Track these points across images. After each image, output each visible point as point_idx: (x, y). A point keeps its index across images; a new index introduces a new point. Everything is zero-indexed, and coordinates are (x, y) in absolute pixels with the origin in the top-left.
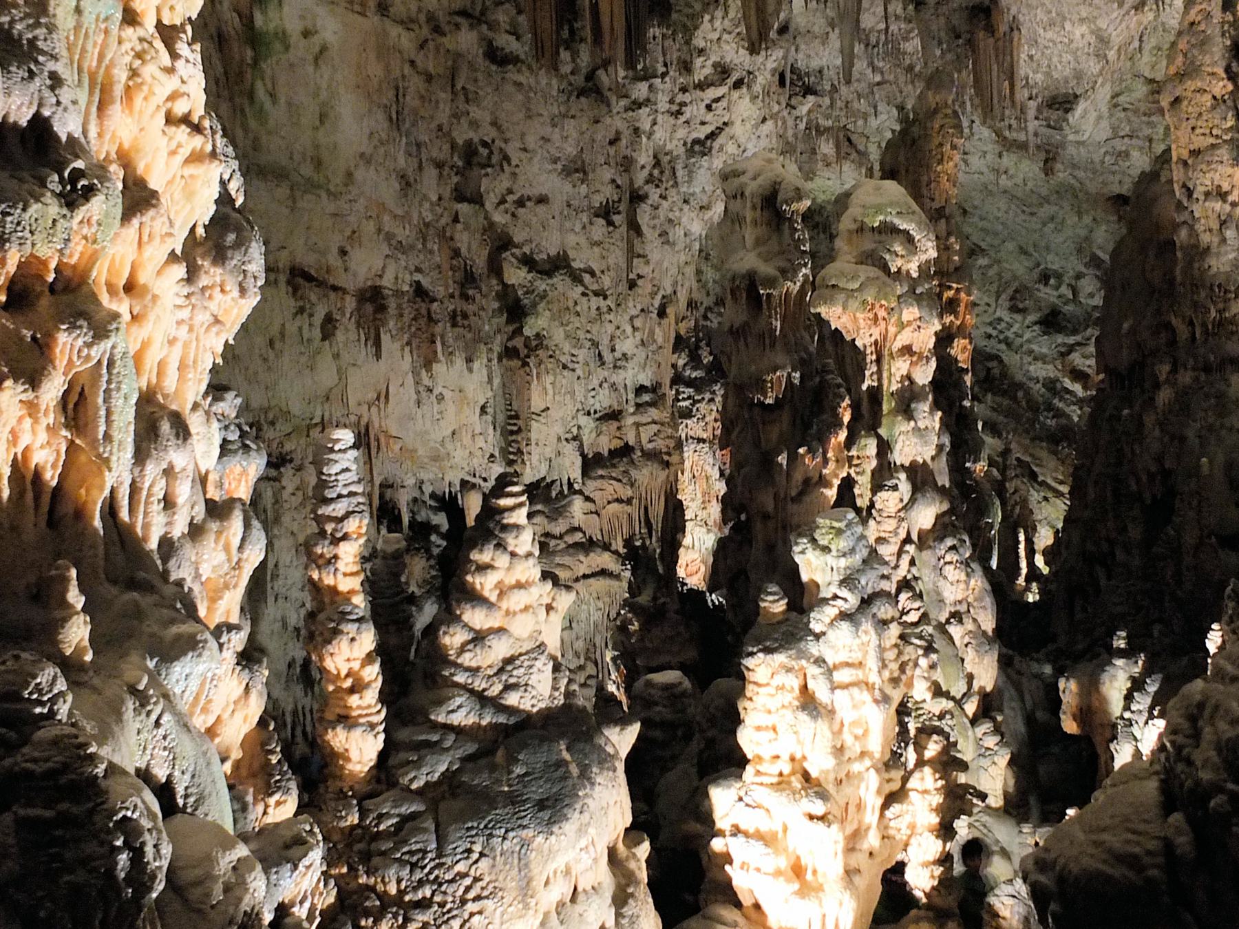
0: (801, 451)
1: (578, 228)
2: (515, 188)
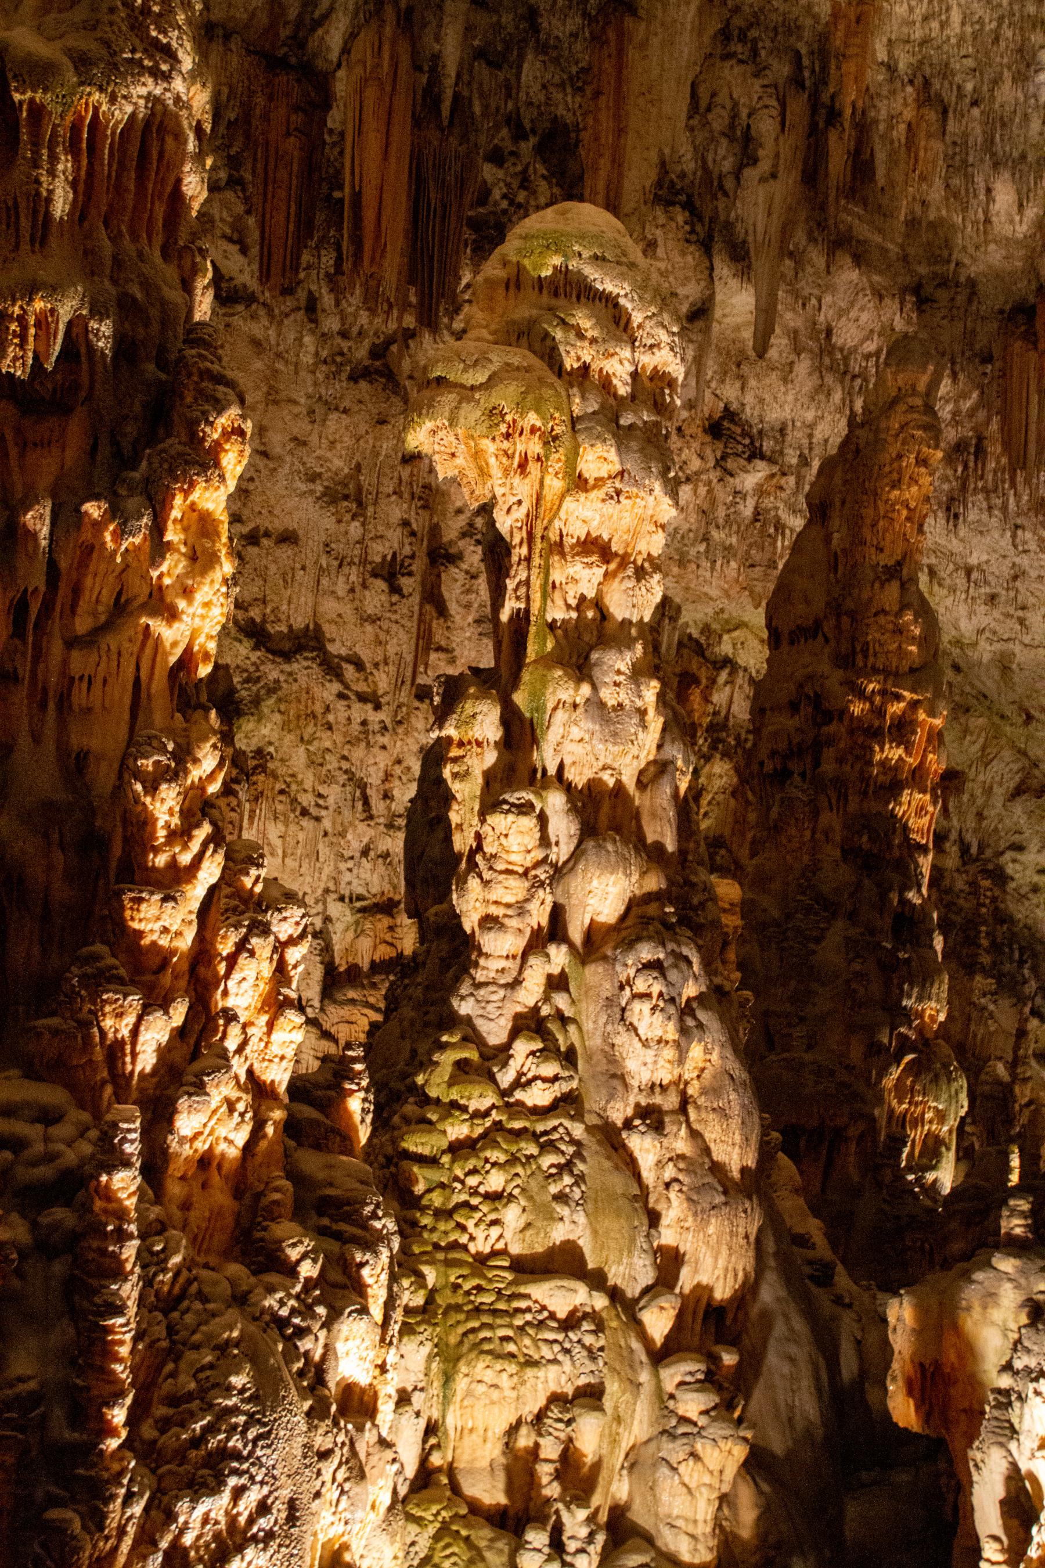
0: (93, 509)
1: (341, 589)
2: (246, 513)
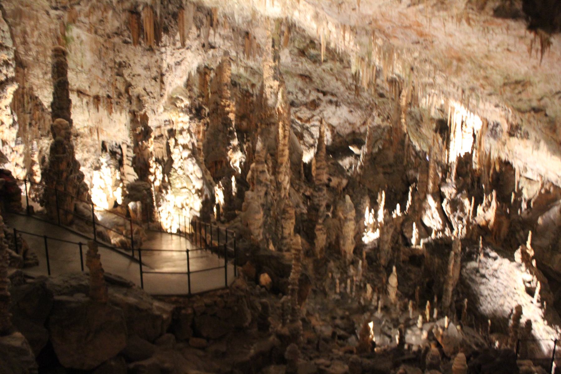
1: (148, 81)
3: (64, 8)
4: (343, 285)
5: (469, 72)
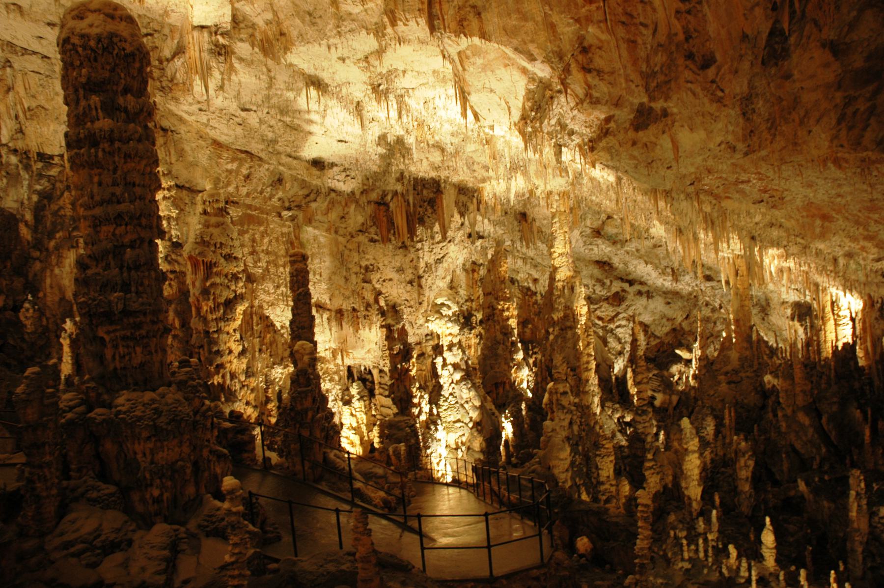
3: (299, 207)
4: (693, 547)
5: (840, 232)
